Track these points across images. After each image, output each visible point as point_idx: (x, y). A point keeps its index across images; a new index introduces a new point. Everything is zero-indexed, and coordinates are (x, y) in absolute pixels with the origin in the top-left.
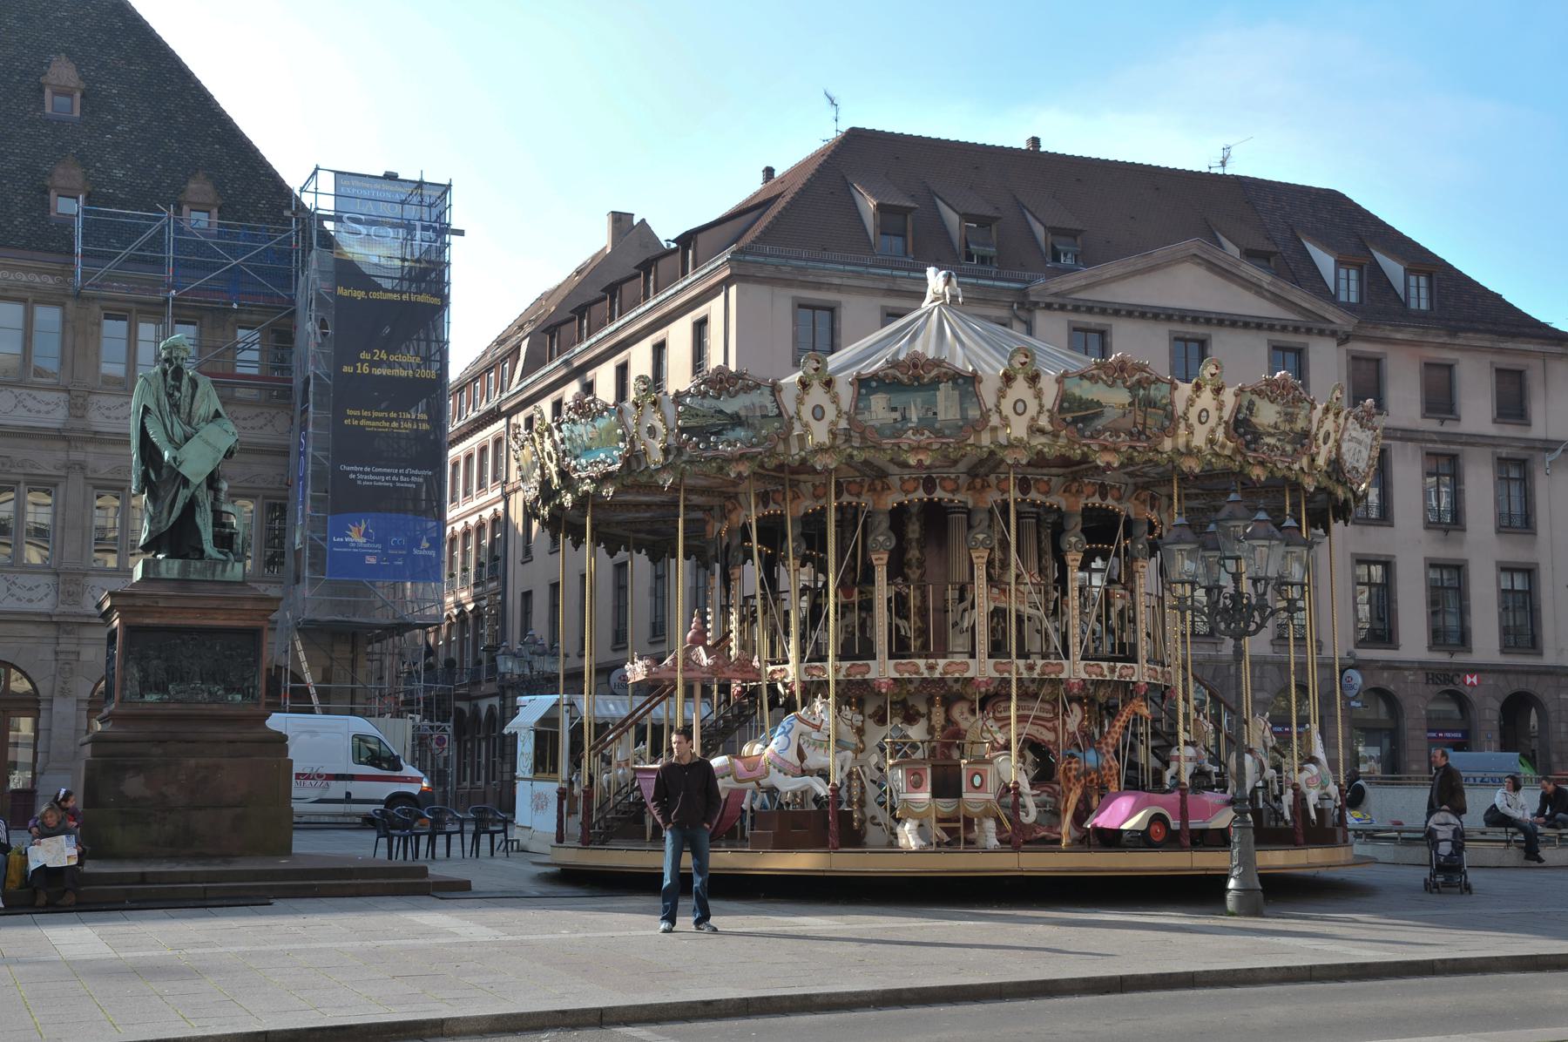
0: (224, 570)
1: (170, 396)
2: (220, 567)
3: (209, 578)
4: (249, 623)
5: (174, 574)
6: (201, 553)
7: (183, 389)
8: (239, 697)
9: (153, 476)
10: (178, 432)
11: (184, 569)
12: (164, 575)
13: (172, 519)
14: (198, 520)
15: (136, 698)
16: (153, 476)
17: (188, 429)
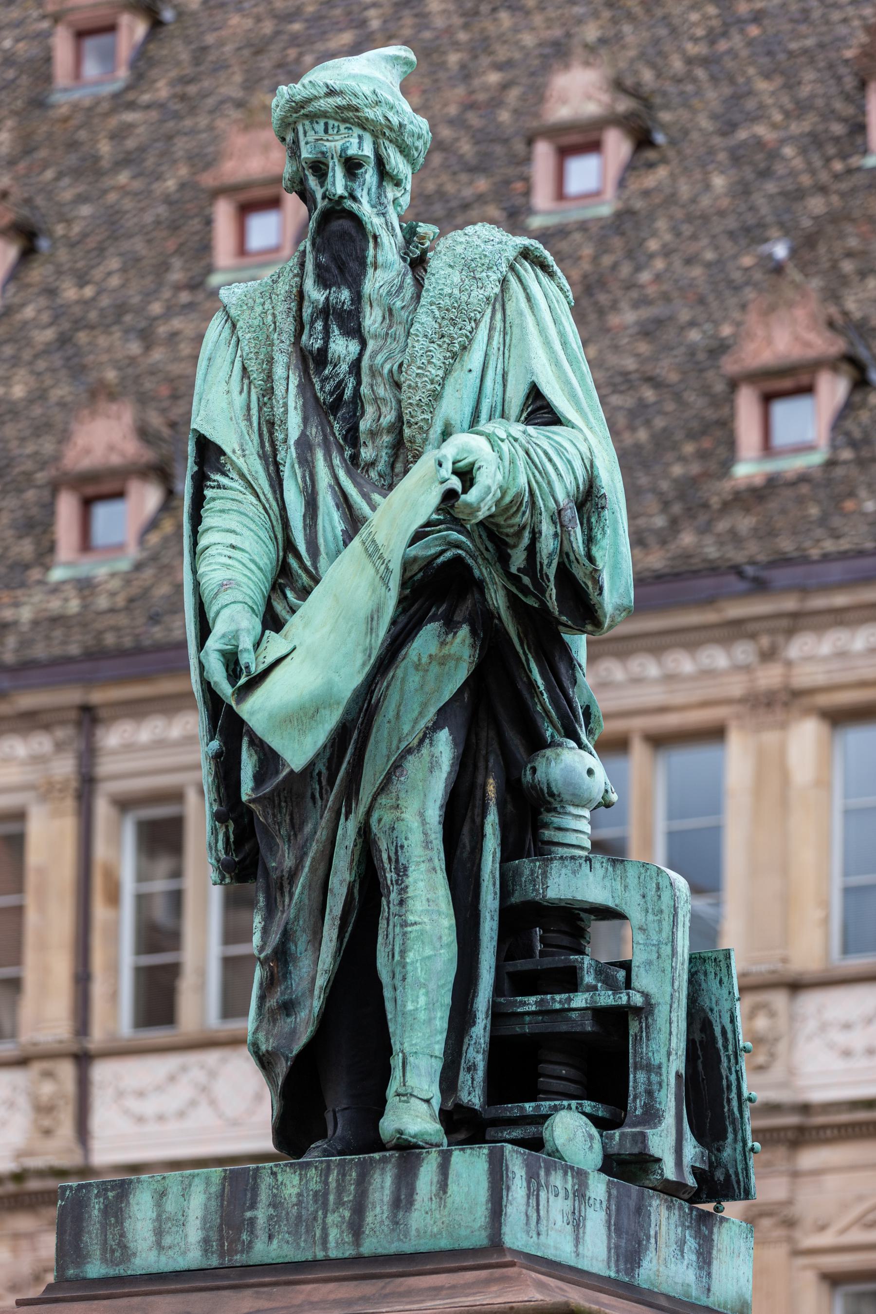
0: (403, 1201)
1: (312, 362)
2: (383, 1184)
3: (338, 1244)
5: (189, 1249)
12: (146, 1258)
13: (321, 981)
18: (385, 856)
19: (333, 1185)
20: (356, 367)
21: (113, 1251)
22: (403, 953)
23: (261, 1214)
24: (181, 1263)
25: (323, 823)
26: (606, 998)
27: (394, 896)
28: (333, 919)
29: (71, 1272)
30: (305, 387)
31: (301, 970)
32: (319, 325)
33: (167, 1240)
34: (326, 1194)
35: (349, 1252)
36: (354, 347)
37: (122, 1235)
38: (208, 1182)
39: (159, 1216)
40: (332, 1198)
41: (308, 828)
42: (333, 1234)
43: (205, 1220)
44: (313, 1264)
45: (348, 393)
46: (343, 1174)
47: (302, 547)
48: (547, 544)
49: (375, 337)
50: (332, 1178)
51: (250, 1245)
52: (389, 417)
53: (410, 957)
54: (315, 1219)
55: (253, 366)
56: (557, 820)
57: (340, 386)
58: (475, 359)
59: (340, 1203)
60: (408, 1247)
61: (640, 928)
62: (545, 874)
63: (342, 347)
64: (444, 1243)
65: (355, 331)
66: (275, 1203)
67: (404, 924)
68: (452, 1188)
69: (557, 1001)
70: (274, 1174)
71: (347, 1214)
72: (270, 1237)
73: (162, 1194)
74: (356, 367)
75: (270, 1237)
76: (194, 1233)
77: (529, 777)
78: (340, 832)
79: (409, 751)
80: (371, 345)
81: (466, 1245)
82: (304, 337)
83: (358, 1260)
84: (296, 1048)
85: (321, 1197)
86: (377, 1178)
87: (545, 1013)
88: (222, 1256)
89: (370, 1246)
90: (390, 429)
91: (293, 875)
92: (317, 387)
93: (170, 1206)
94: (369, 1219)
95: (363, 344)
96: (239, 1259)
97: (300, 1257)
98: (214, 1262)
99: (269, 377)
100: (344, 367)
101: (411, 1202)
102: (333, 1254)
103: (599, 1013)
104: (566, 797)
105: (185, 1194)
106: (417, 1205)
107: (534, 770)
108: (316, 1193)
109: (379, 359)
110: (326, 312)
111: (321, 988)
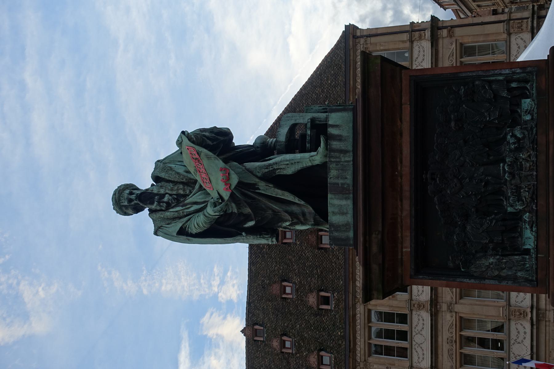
0: (339, 138)
2: (335, 144)
3: (349, 158)
4: (405, 98)
5: (348, 204)
6: (323, 167)
7: (162, 191)
8: (527, 103)
9: (251, 224)
10: (197, 197)
11: (341, 191)
12: (349, 218)
13: (297, 200)
14: (290, 171)
15: (530, 261)
16: (251, 224)
17: (197, 187)
18: (266, 170)
19: (334, 160)
20: (171, 195)
21: (347, 228)
22: (287, 161)
23: (340, 181)
24: (351, 206)
25: (261, 199)
26: (309, 125)
27: (275, 167)
28: (283, 195)
29: (352, 242)
30: (173, 208)
31: (295, 209)
32: (161, 204)
33: (345, 211)
34: (337, 162)
35: (351, 154)
36: (167, 195)
37: (343, 225)
38: (331, 198)
39: (339, 214)
40: (338, 160)
41: (263, 206)
42: (347, 159)
43: (340, 199)
44: (353, 164)
45: (175, 197)
46: (332, 157)
47: (203, 205)
48: (207, 134)
49: (166, 190)
50: (333, 160)
51: (348, 185)
52: (181, 186)
53: (288, 159)
54: (342, 165)
55: (167, 222)
56: (269, 143)
57: (174, 199)
58: (173, 166)
59: (339, 157)
60: (352, 136)
61: (296, 120)
62: (280, 142)
63: (166, 199)
64: (351, 125)
65: (163, 196)
66: (338, 177)
67: (281, 161)
68: (337, 123)
69: (308, 138)
70: (331, 178)
71: (342, 155)
72: (346, 178)
73: (333, 212)
74: (171, 195)
75: (346, 178)
76: (344, 202)
77: (259, 149)
78: (263, 192)
79: (245, 168)
80: (167, 191)
81: (352, 118)
82: (163, 209)
83: (353, 151)
84: (313, 211)
85: (337, 163)
86: (334, 147)
87: (311, 142)
88: (350, 193)
89: (350, 148)
90: (184, 186)
91: (274, 211)
92: (173, 205)
93: (336, 210)
94: (343, 148)
95: (167, 193)
96: (351, 188)
97: (352, 169)
98: (351, 196)
99: (171, 219)
100: (170, 197)
101: (340, 136)
102: (352, 159)
103: (312, 128)
104: (265, 140)
105: (334, 205)
106: (341, 134)
107: (258, 147)
108: (336, 165)
109: (169, 188)
110: (159, 202)
111: (299, 200)
